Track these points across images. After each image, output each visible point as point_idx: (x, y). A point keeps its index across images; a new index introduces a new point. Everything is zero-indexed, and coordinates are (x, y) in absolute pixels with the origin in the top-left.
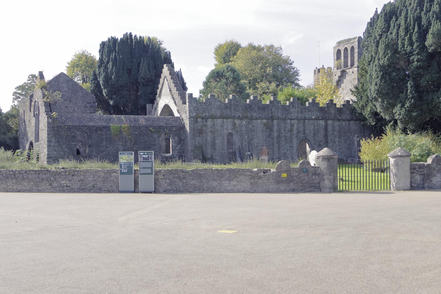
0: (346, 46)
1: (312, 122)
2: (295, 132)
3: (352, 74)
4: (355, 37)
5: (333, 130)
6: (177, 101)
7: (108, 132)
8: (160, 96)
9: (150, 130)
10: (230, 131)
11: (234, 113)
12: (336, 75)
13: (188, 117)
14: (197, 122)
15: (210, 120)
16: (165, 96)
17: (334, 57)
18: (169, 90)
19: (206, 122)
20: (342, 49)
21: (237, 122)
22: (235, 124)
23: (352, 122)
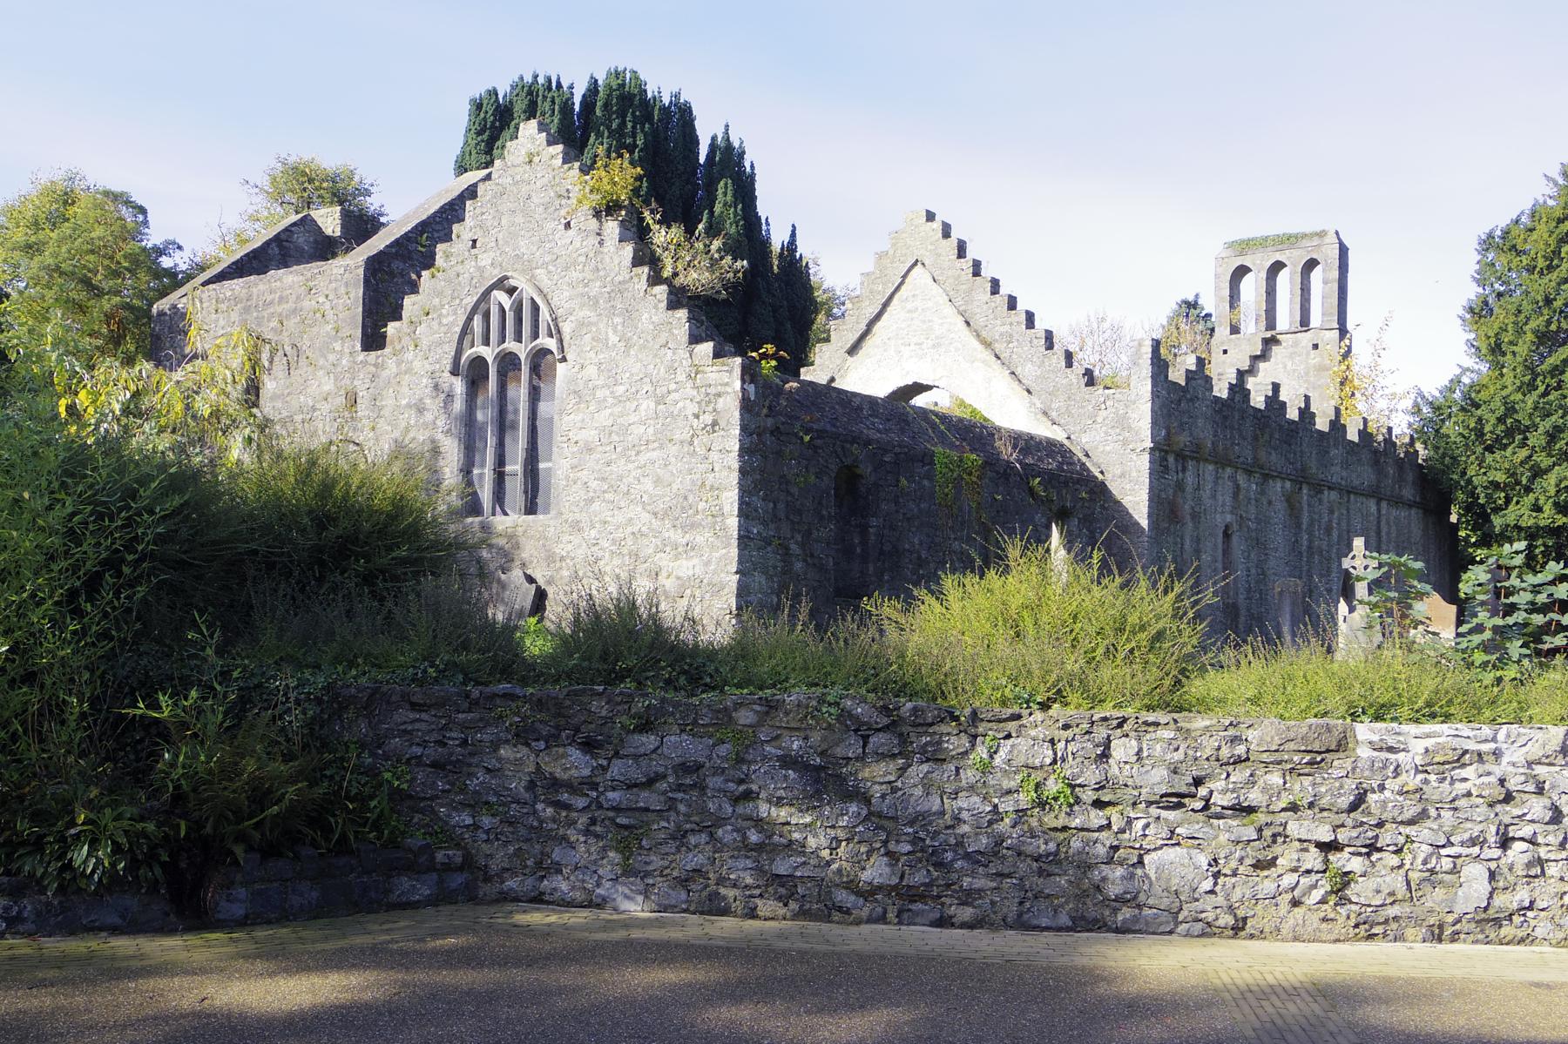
0: (1279, 257)
1: (1360, 499)
2: (1335, 534)
3: (1308, 354)
4: (1318, 229)
5: (1388, 533)
6: (1028, 371)
7: (926, 482)
8: (853, 350)
9: (1031, 491)
10: (1229, 518)
11: (1238, 444)
12: (1225, 352)
13: (1149, 444)
14: (1166, 469)
15: (1190, 464)
16: (902, 348)
17: (1217, 288)
18: (960, 321)
19: (1184, 470)
20: (1259, 263)
21: (1241, 478)
22: (1238, 487)
23: (1413, 511)
